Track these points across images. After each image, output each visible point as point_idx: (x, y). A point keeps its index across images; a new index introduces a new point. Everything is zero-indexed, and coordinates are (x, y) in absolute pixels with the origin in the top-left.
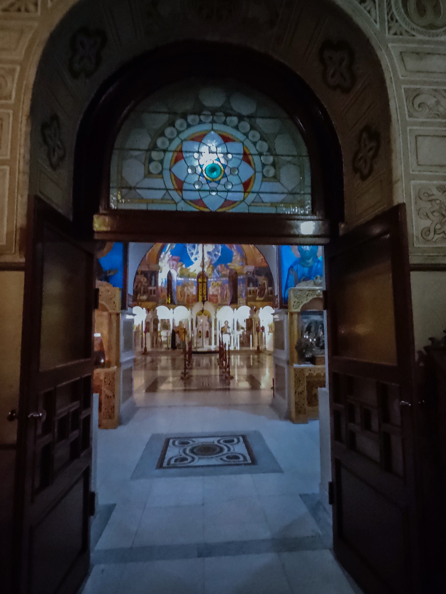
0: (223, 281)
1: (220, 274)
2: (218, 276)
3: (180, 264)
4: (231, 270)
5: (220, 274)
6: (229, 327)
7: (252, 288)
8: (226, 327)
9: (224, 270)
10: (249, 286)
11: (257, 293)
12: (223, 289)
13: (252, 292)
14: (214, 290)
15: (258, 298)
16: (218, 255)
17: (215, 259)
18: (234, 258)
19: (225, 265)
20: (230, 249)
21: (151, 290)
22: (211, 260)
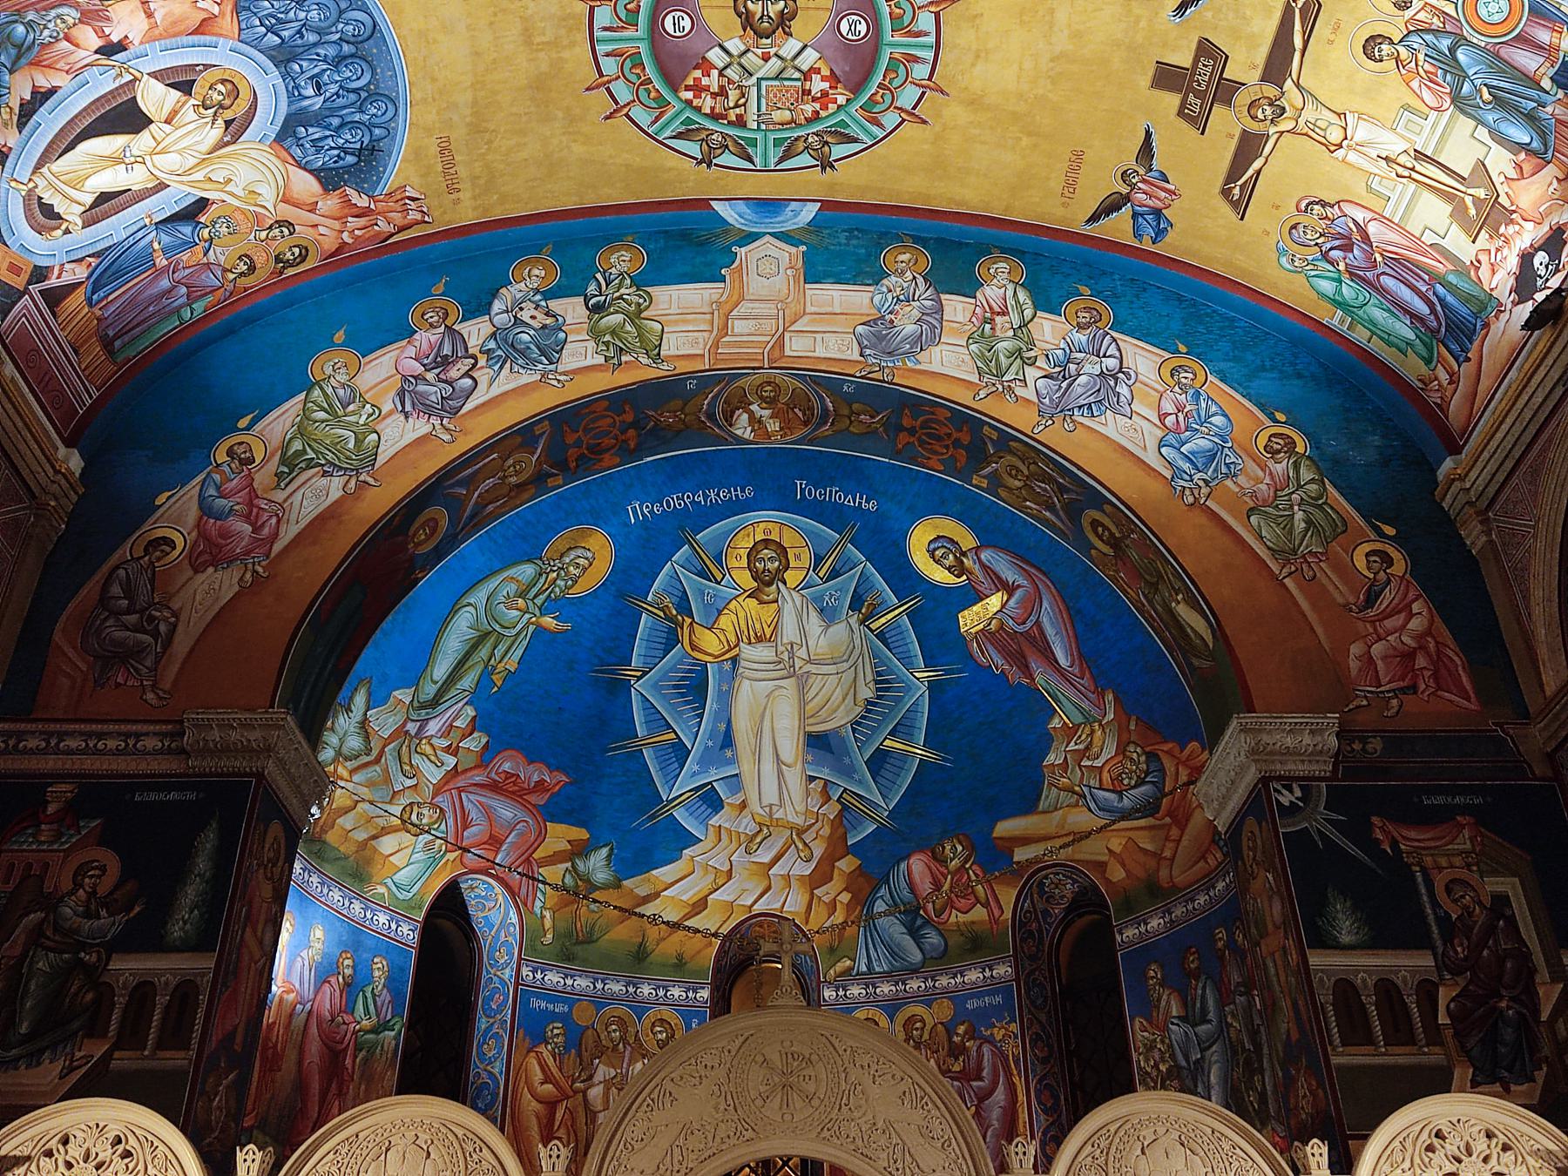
0: (957, 997)
1: (933, 938)
2: (916, 956)
3: (560, 835)
4: (1033, 880)
5: (933, 938)
7: (1367, 964)
9: (965, 890)
10: (1323, 941)
11: (1443, 1019)
13: (1369, 1001)
16: (905, 757)
17: (882, 801)
18: (1051, 758)
19: (971, 847)
20: (1015, 676)
21: (143, 991)
22: (847, 814)
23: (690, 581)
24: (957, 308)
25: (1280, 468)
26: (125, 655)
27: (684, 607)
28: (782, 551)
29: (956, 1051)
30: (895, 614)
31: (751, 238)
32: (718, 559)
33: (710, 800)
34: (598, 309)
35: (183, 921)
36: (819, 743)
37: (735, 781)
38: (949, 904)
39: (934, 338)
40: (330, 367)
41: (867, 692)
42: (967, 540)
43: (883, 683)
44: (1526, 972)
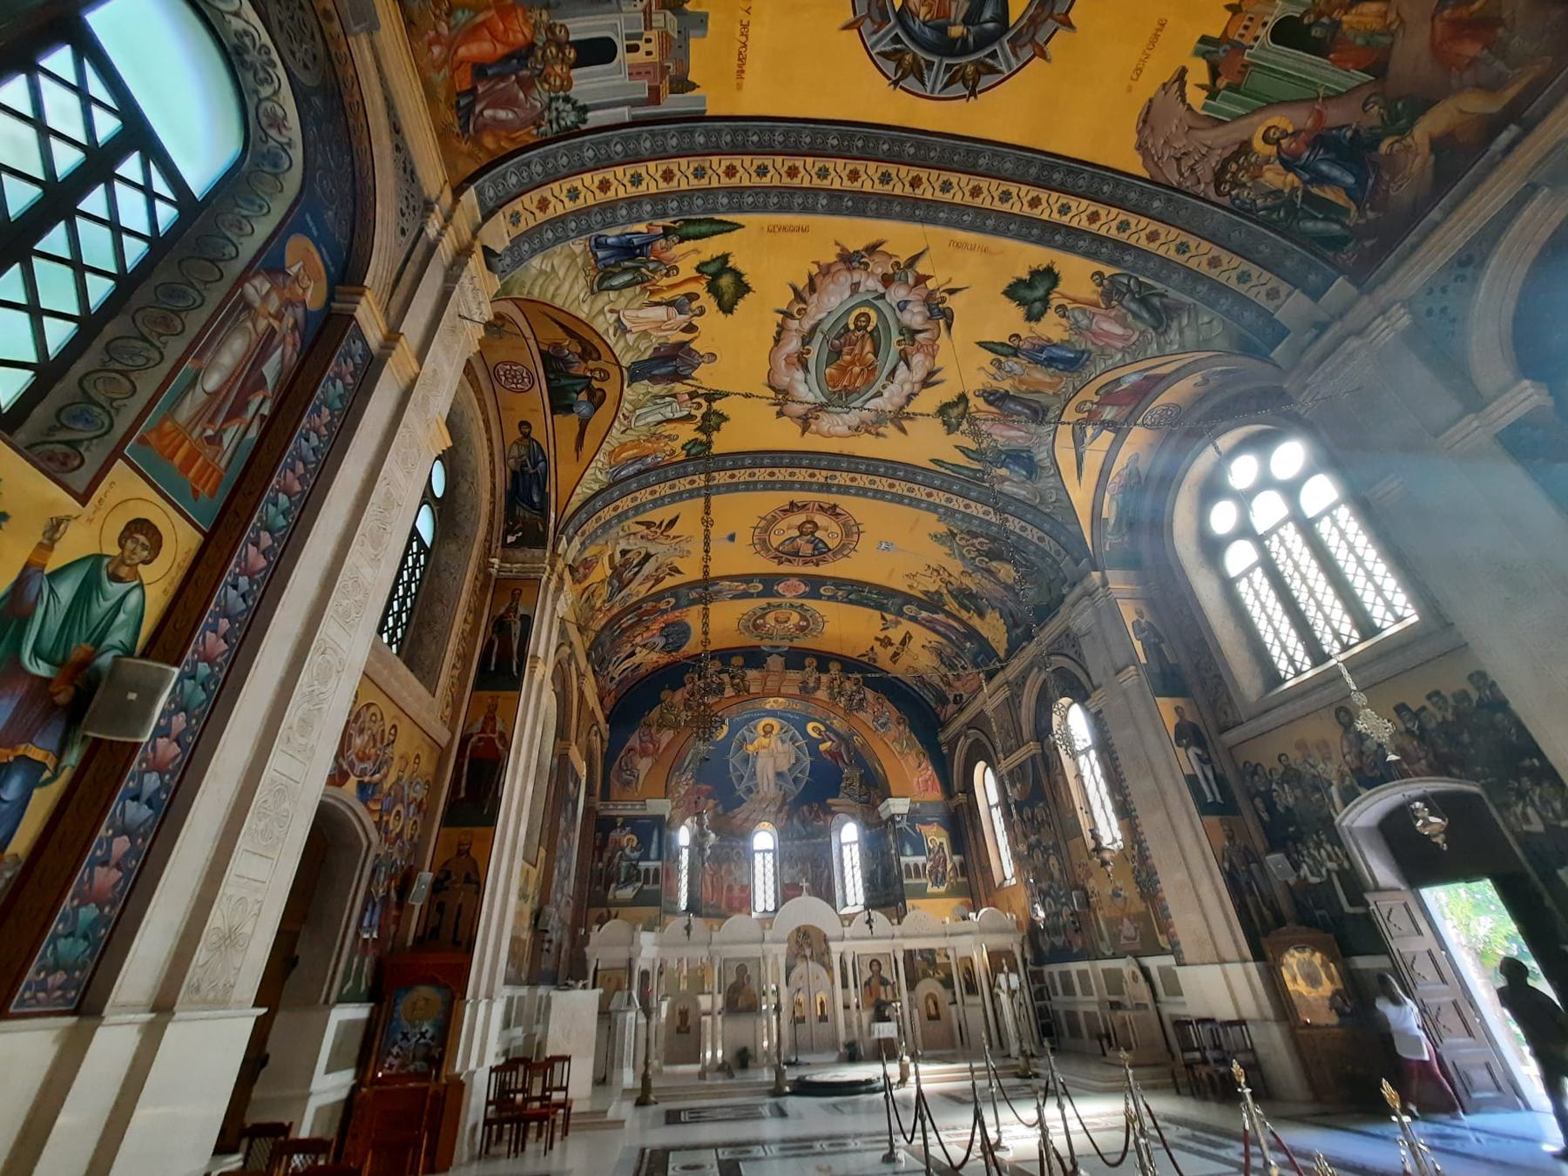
6: (884, 982)
8: (874, 982)
12: (819, 867)
14: (791, 871)
15: (930, 889)
18: (843, 785)
23: (746, 733)
24: (824, 678)
25: (901, 728)
26: (628, 783)
27: (745, 740)
28: (772, 727)
29: (815, 860)
30: (802, 742)
31: (770, 654)
32: (755, 728)
33: (749, 790)
34: (732, 678)
35: (653, 853)
36: (779, 775)
37: (756, 785)
38: (814, 819)
39: (818, 688)
40: (664, 695)
41: (793, 761)
42: (823, 728)
43: (797, 759)
44: (945, 861)
